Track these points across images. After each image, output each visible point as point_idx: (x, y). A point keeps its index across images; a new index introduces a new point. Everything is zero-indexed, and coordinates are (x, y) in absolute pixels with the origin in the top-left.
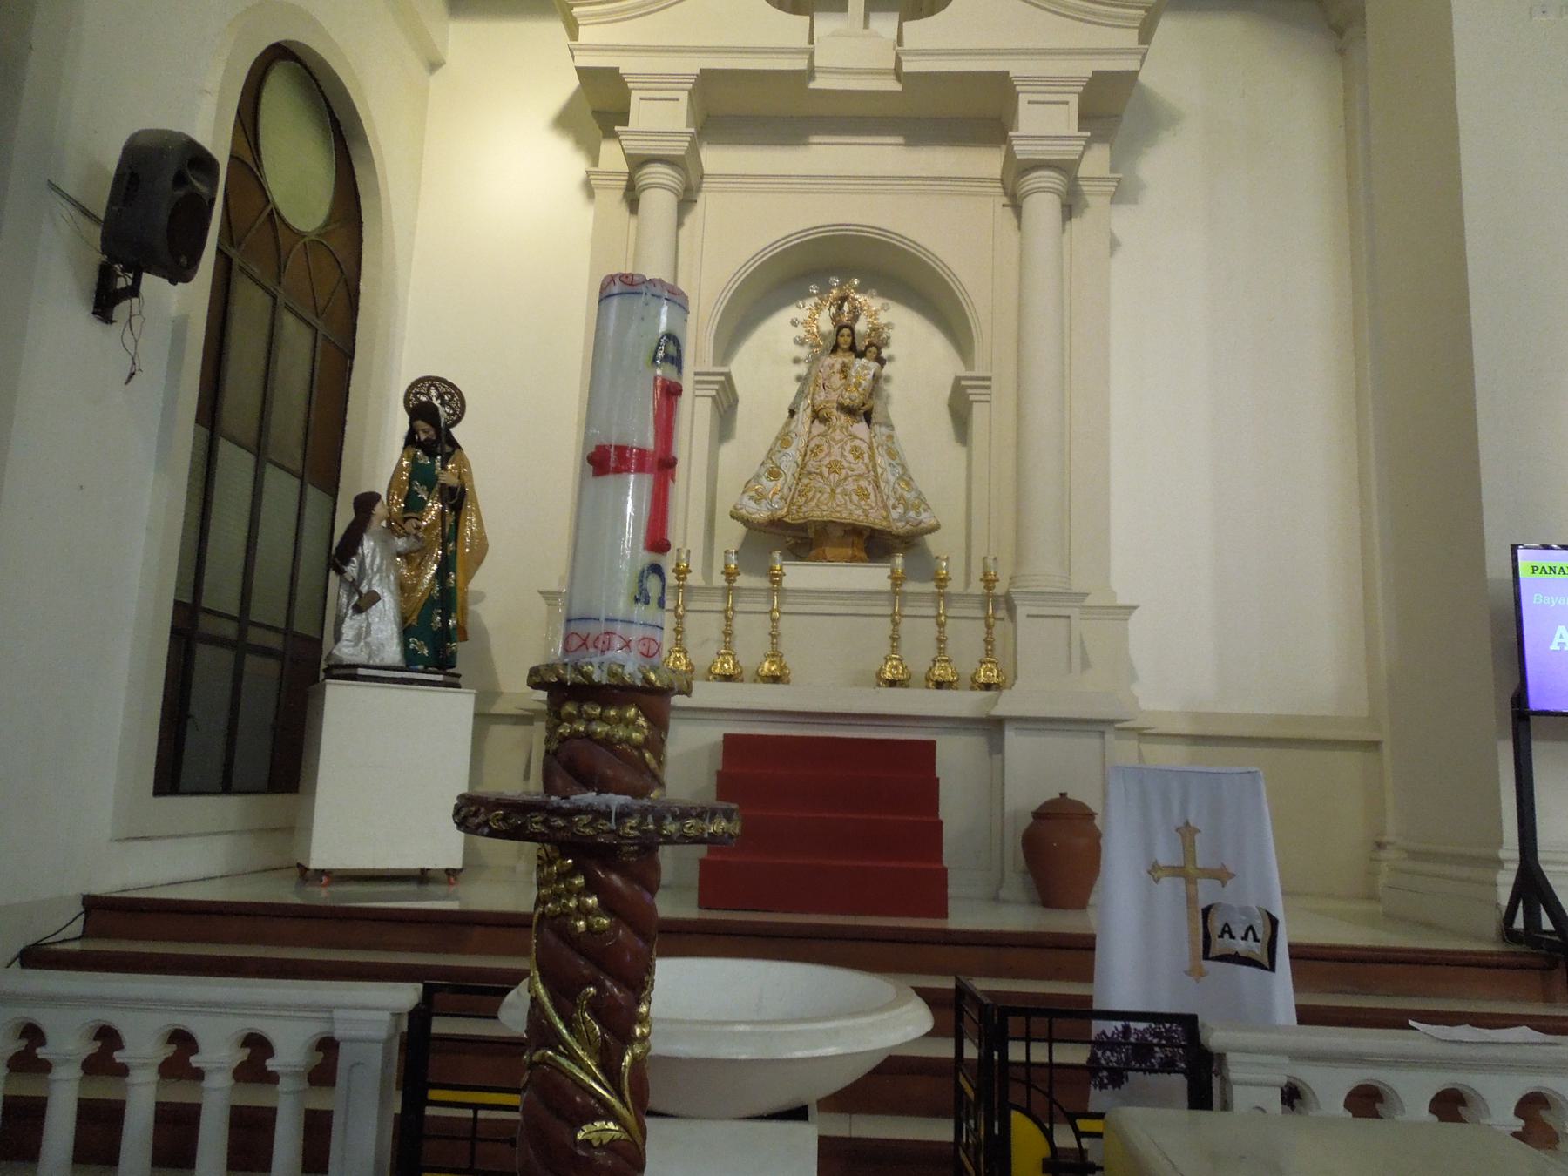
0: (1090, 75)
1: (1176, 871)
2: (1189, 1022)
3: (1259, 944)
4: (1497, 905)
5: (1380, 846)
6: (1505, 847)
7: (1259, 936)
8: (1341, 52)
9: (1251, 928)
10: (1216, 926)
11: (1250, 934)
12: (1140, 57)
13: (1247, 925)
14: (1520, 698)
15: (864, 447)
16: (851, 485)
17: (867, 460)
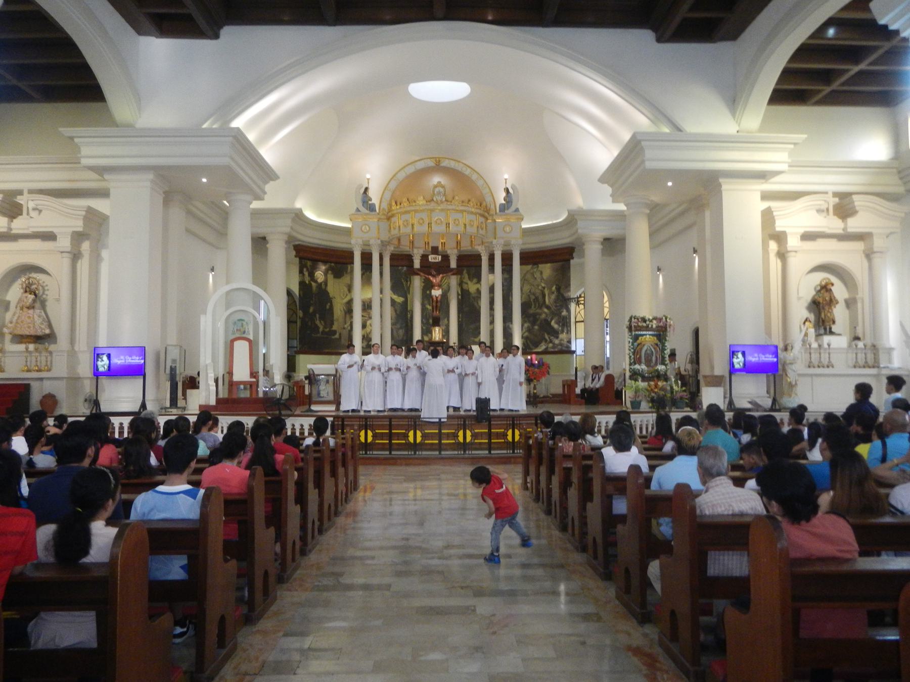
15: (31, 315)
16: (25, 326)
17: (32, 319)
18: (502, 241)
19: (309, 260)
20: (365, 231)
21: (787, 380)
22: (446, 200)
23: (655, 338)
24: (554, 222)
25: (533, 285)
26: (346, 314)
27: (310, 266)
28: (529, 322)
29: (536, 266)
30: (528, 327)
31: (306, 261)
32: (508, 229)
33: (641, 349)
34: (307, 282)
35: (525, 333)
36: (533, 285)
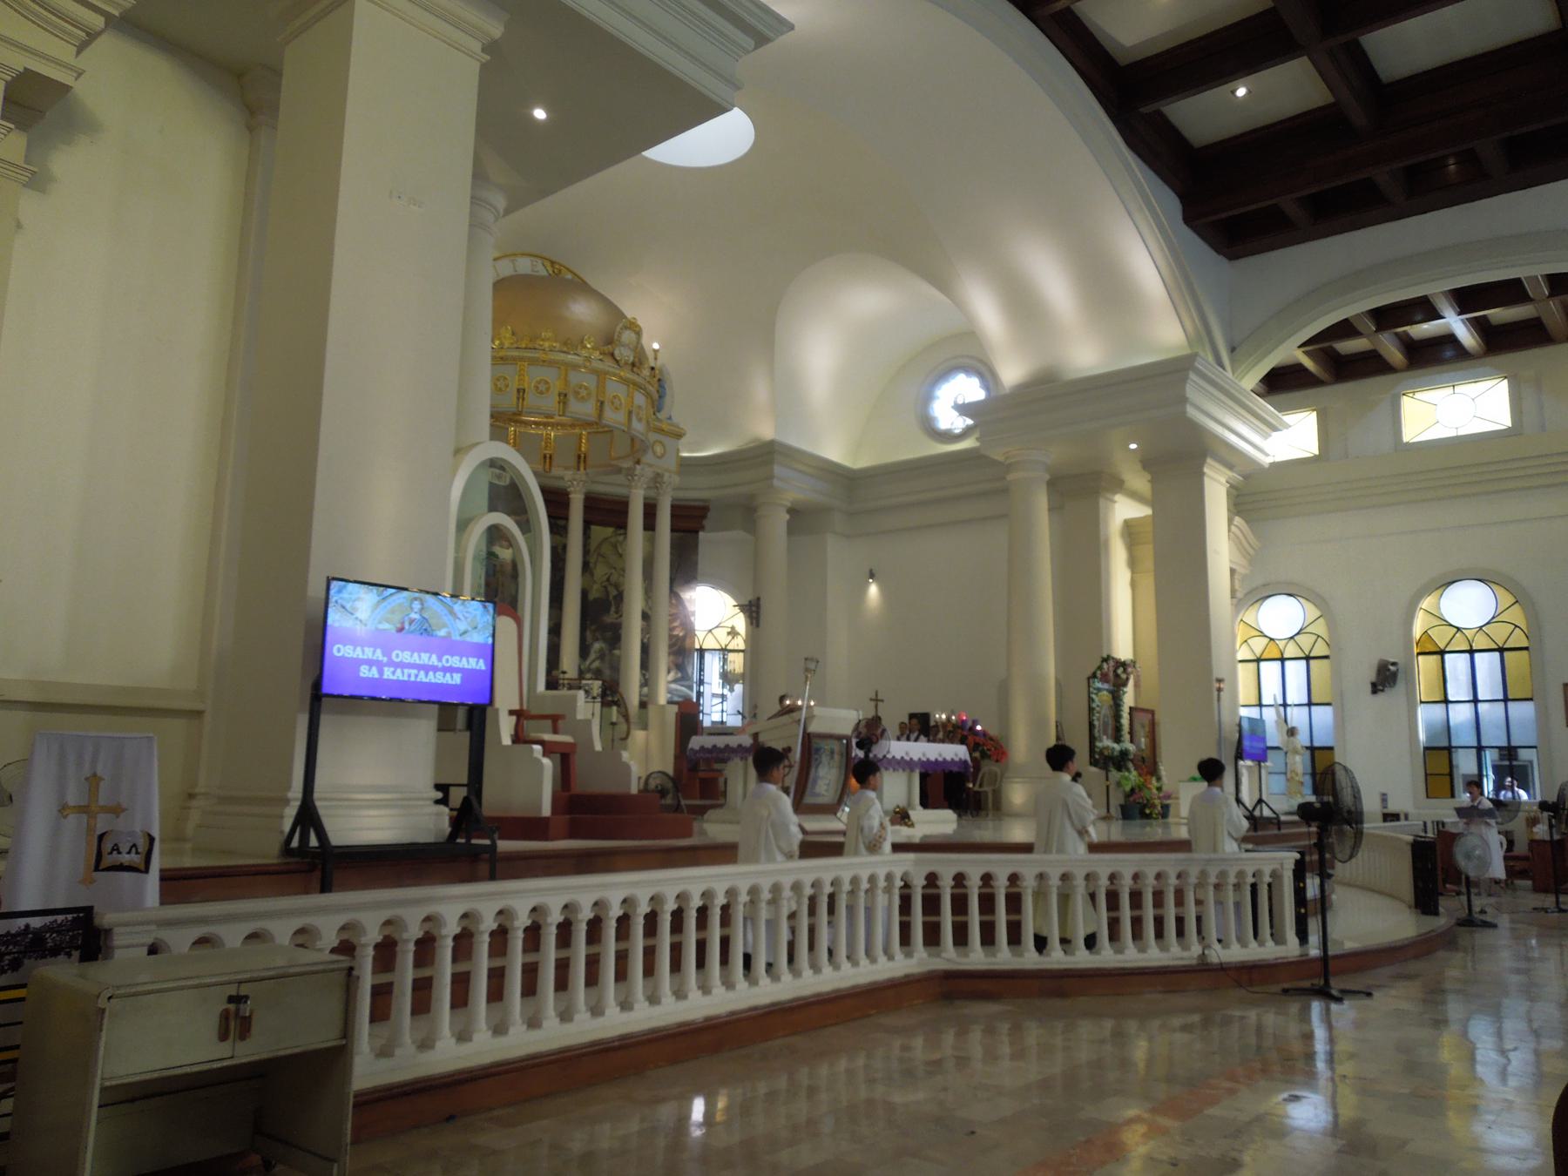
0: (21, 70)
1: (82, 809)
2: (89, 910)
3: (139, 856)
4: (282, 832)
5: (191, 796)
6: (292, 790)
7: (139, 850)
8: (251, 129)
9: (134, 845)
10: (107, 846)
11: (134, 850)
12: (75, 75)
13: (131, 844)
14: (317, 685)
18: (649, 472)
22: (633, 365)
23: (1110, 696)
25: (615, 568)
28: (605, 640)
29: (622, 531)
30: (601, 650)
32: (659, 449)
35: (594, 661)
36: (615, 568)
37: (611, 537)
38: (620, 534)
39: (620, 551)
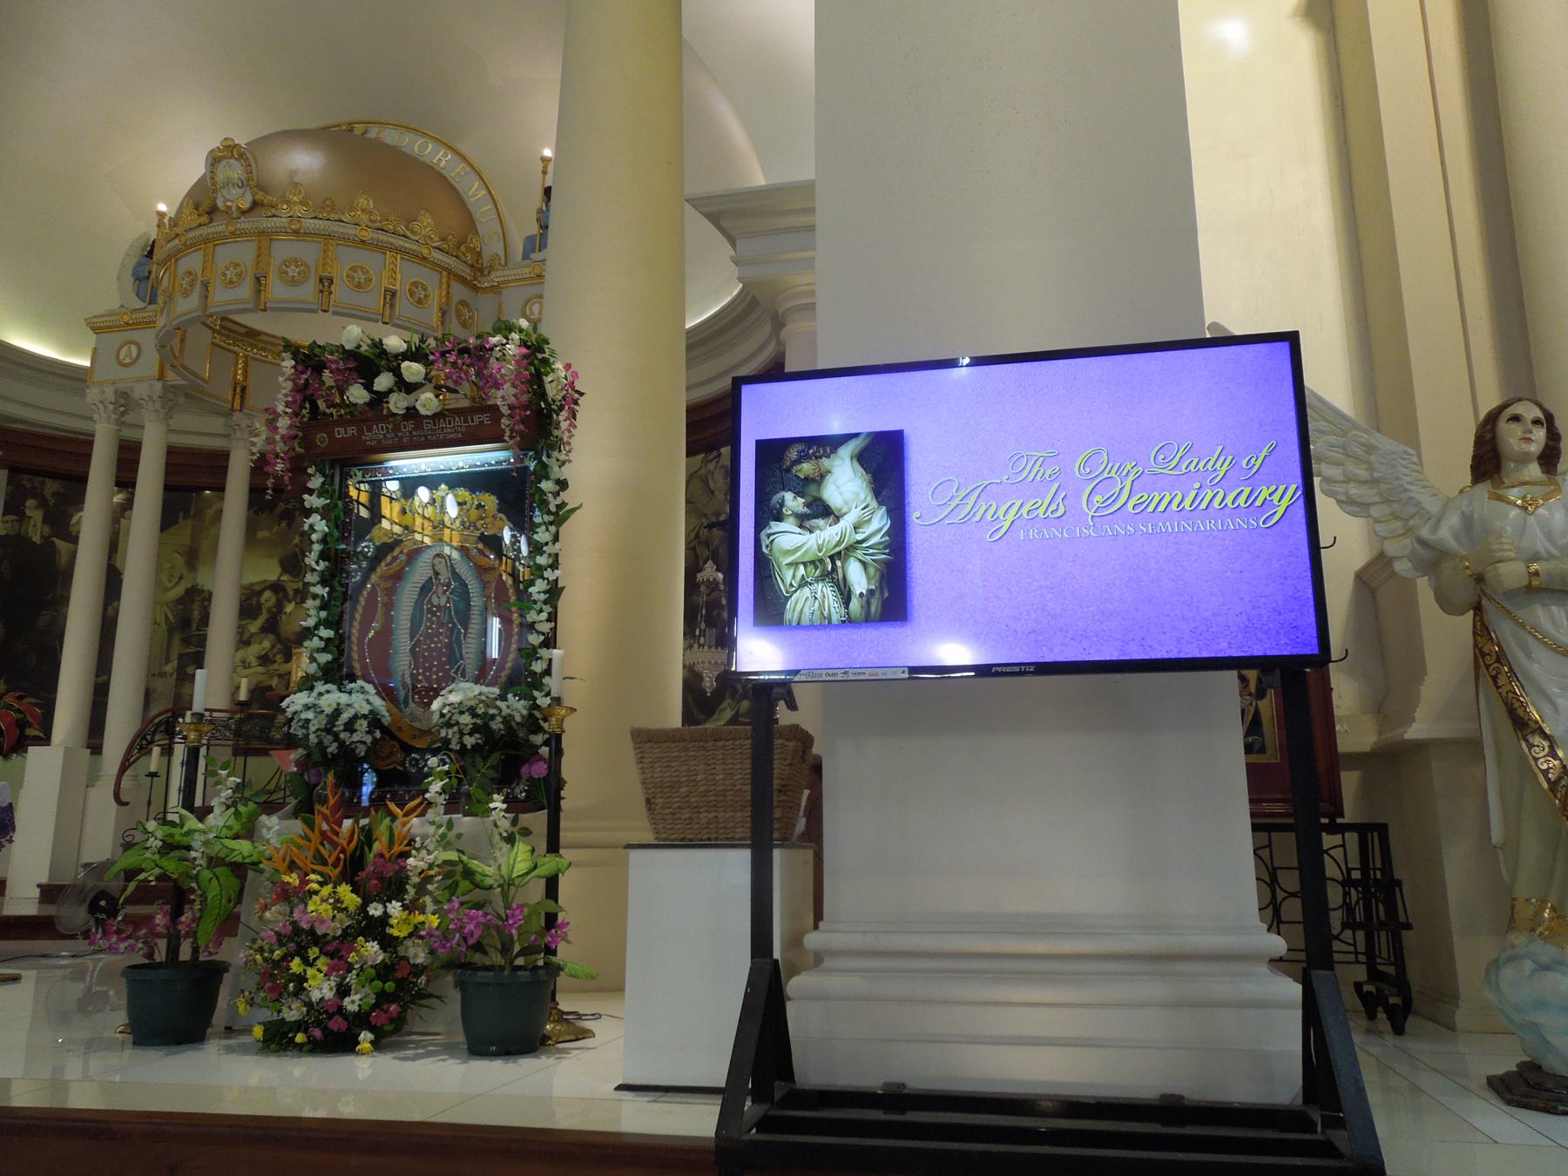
19: (54, 476)
20: (128, 360)
21: (1525, 768)
22: (255, 205)
23: (490, 501)
24: (735, 293)
26: (171, 631)
27: (54, 494)
29: (715, 453)
31: (40, 479)
33: (399, 576)
34: (37, 539)
37: (700, 469)
38: (711, 460)
39: (712, 486)
